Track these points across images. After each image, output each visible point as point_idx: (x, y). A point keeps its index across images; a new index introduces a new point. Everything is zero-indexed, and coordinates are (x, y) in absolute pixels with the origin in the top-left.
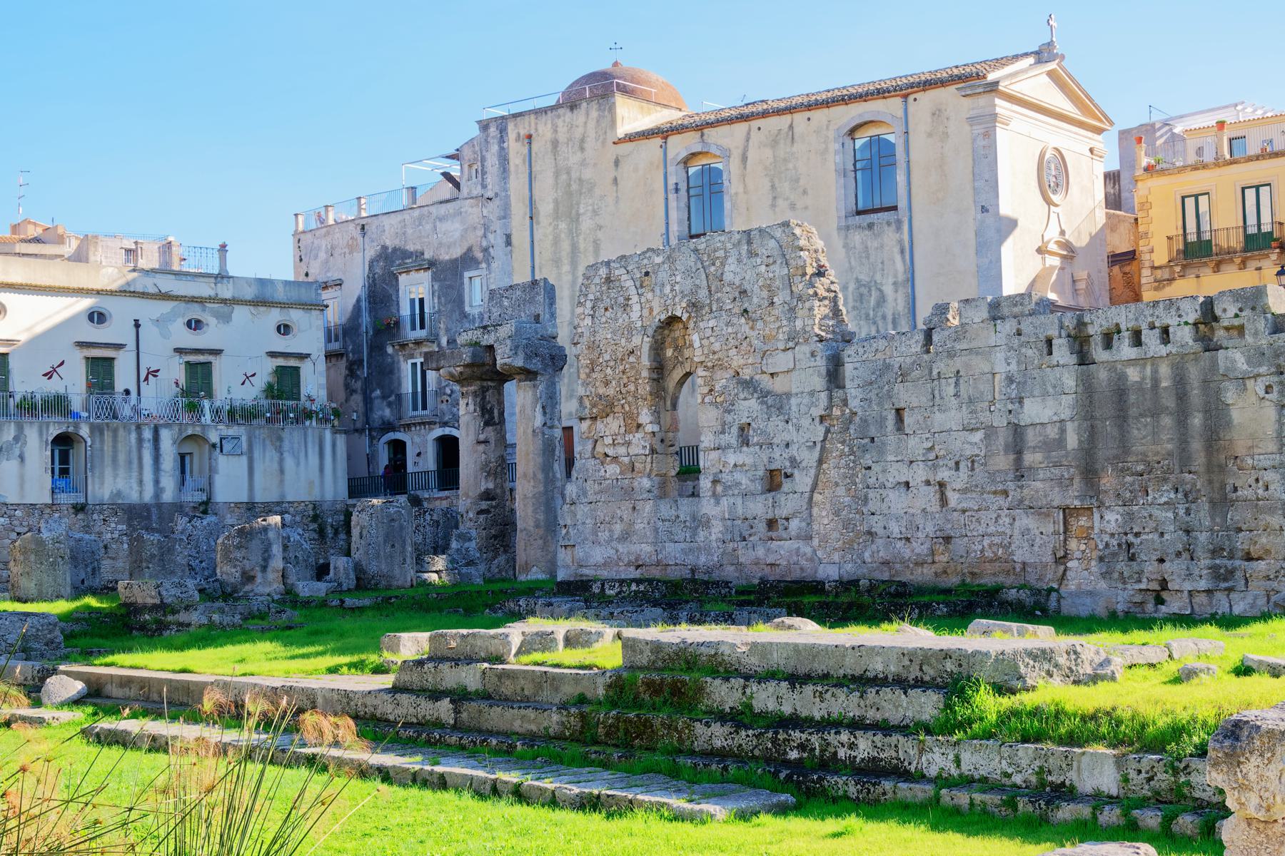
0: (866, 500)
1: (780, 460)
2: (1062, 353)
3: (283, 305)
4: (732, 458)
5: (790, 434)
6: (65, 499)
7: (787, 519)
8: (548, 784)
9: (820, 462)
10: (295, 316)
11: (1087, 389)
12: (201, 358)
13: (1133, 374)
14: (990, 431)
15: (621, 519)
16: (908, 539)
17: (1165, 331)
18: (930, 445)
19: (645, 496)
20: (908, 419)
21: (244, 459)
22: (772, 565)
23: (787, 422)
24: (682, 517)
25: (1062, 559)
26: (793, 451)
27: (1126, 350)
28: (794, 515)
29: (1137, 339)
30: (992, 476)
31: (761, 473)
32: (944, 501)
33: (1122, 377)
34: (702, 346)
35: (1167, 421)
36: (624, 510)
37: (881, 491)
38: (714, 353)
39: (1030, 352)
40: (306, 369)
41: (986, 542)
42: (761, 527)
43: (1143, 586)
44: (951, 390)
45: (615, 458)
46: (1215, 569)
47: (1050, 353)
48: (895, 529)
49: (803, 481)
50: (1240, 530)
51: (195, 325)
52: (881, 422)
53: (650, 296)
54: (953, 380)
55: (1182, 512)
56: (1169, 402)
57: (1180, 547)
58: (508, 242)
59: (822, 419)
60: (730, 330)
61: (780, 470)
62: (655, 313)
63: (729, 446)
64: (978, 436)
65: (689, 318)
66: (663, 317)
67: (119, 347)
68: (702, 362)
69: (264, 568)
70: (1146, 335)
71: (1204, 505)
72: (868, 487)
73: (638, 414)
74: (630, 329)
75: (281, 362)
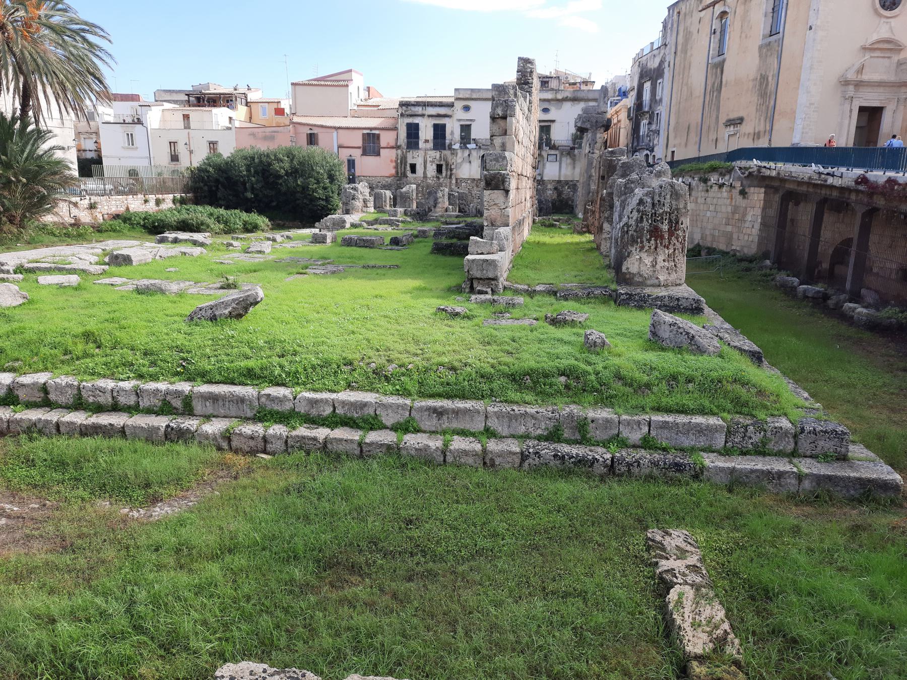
58: (669, 66)
69: (435, 207)
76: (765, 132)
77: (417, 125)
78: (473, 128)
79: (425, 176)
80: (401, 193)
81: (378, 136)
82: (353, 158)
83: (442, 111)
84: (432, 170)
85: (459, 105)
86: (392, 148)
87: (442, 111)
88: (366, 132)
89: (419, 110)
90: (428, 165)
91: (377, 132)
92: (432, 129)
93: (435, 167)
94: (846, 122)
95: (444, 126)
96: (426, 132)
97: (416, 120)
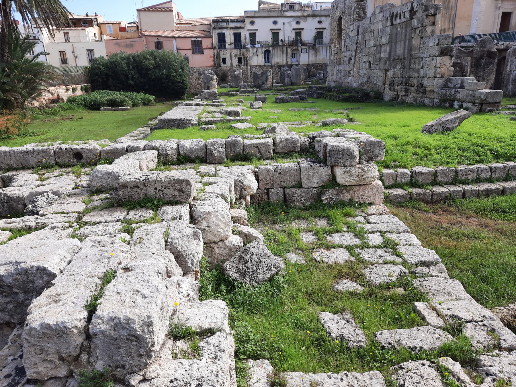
2: (389, 23)
3: (320, 16)
6: (267, 64)
9: (355, 55)
10: (323, 19)
12: (299, 31)
17: (405, 13)
21: (307, 54)
25: (385, 84)
27: (398, 21)
35: (403, 43)
40: (325, 32)
46: (405, 89)
51: (298, 23)
56: (403, 37)
59: (357, 43)
67: (280, 29)
69: (266, 81)
75: (319, 30)
76: (449, 28)
77: (224, 33)
78: (257, 34)
79: (232, 65)
80: (235, 75)
81: (201, 41)
82: (187, 56)
83: (238, 25)
84: (235, 61)
85: (248, 21)
86: (210, 48)
87: (238, 25)
88: (193, 39)
89: (224, 24)
90: (233, 58)
91: (200, 39)
92: (233, 36)
93: (237, 59)
94: (497, 21)
95: (240, 34)
96: (230, 39)
97: (223, 31)
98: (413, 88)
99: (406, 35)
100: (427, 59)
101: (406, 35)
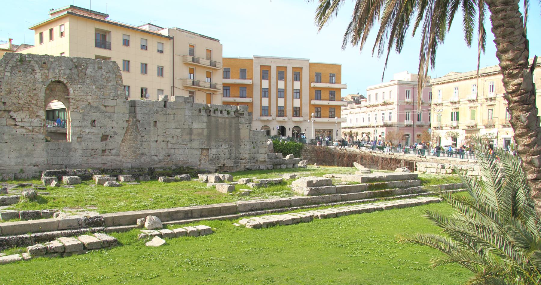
0: (141, 145)
1: (109, 131)
2: (203, 113)
4: (87, 131)
5: (114, 124)
7: (111, 150)
8: (190, 228)
9: (125, 134)
11: (209, 123)
13: (220, 120)
14: (183, 129)
15: (27, 149)
16: (156, 156)
18: (165, 131)
19: (40, 141)
20: (158, 124)
22: (103, 164)
23: (113, 121)
24: (62, 149)
26: (115, 130)
28: (114, 149)
29: (221, 112)
30: (183, 141)
31: (101, 136)
32: (167, 146)
33: (218, 120)
34: (74, 93)
35: (227, 131)
36: (30, 146)
37: (148, 143)
38: (80, 96)
39: (195, 112)
41: (181, 156)
42: (100, 152)
43: (219, 166)
44: (173, 118)
45: (22, 127)
47: (200, 112)
48: (152, 153)
49: (118, 139)
50: (241, 154)
52: (149, 124)
53: (46, 71)
54: (173, 115)
55: (230, 150)
57: (229, 157)
60: (88, 89)
61: (107, 136)
62: (49, 78)
63: (86, 127)
64: (179, 130)
65: (67, 83)
66: (53, 80)
68: (73, 98)
70: (223, 112)
71: (234, 148)
72: (143, 141)
73: (37, 112)
74: (35, 81)
98: (244, 161)
99: (230, 126)
100: (258, 143)
101: (230, 126)
